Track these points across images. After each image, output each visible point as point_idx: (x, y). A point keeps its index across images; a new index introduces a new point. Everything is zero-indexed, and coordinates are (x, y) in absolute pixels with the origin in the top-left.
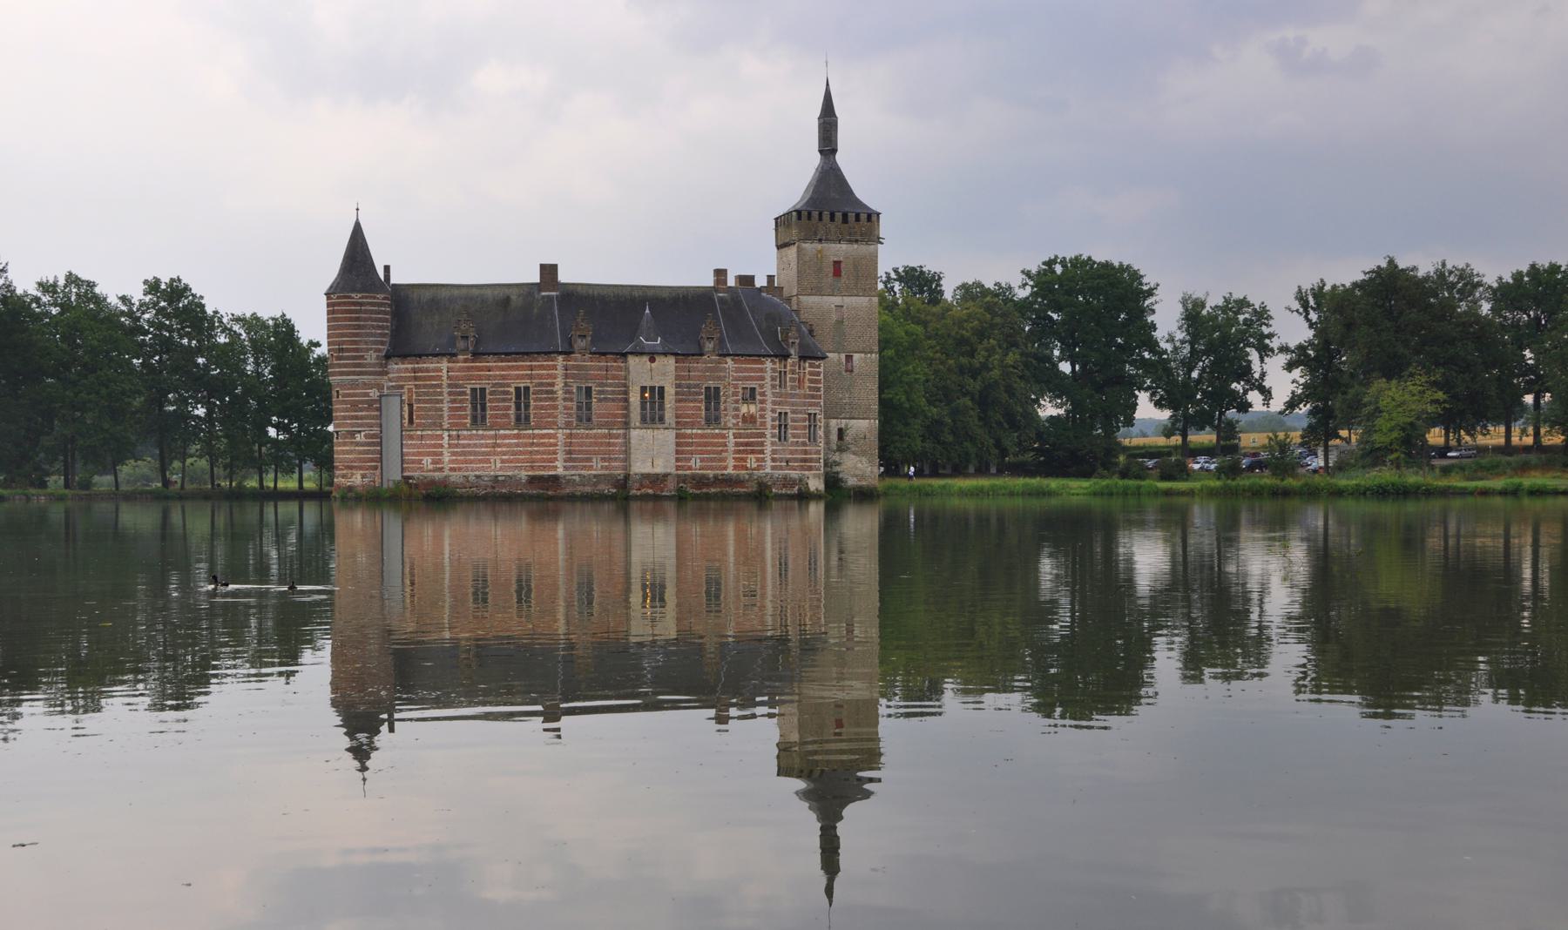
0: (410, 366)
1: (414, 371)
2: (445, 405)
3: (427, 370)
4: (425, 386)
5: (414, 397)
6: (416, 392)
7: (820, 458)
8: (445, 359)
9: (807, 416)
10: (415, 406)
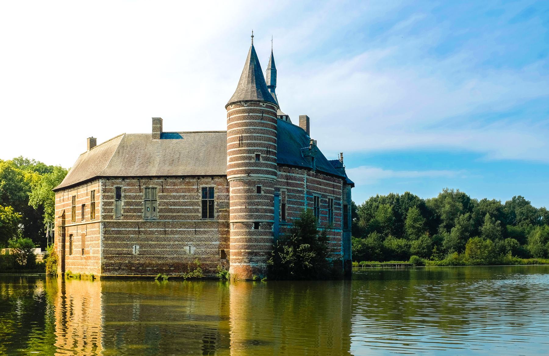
0: (284, 173)
1: (287, 178)
2: (305, 207)
3: (295, 179)
4: (294, 191)
5: (286, 199)
6: (288, 195)
8: (306, 172)
10: (287, 206)
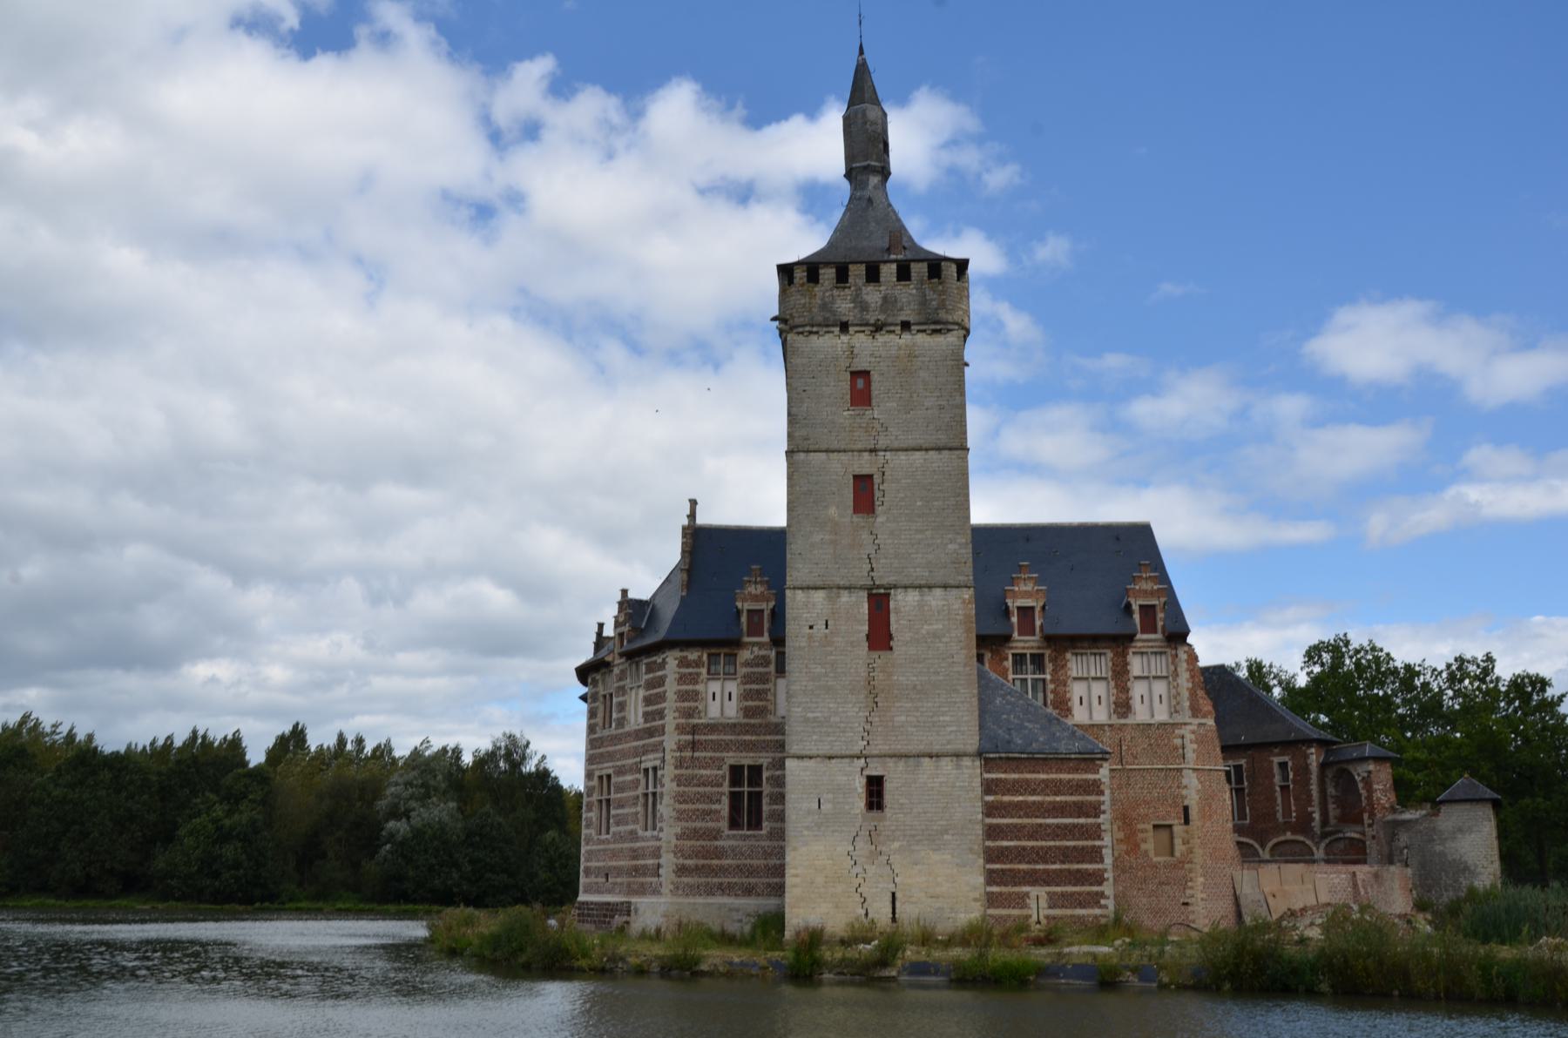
7: (659, 866)
9: (641, 776)
